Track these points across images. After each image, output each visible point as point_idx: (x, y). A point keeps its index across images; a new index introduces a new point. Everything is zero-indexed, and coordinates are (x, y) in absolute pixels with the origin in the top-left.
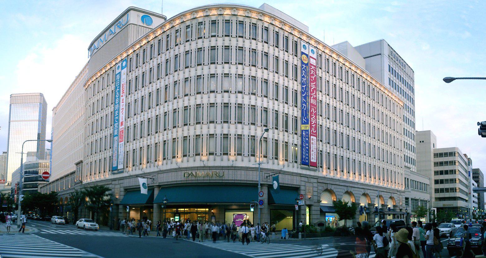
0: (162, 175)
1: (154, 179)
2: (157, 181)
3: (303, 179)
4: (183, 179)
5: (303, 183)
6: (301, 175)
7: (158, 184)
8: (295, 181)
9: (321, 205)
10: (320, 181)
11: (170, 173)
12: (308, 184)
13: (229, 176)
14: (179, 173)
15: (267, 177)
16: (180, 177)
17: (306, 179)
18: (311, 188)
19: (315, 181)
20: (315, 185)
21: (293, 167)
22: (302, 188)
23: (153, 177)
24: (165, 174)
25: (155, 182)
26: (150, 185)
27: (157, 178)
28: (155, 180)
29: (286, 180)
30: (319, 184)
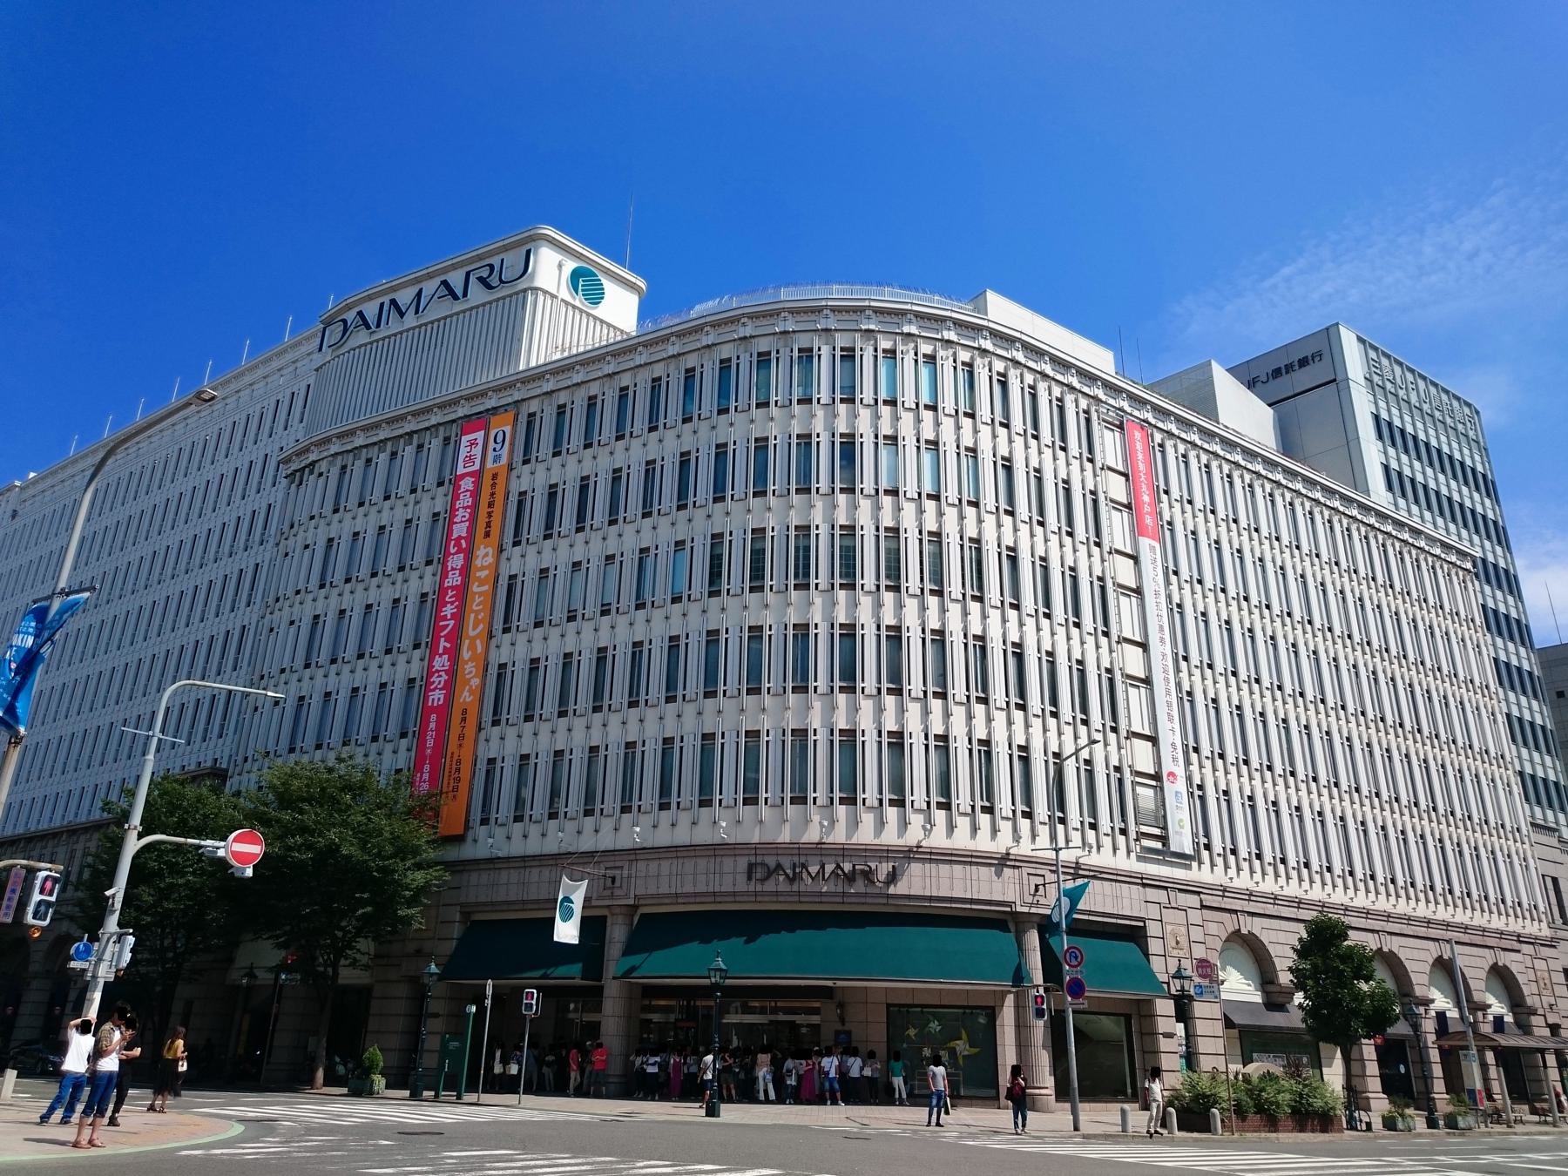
0: (653, 865)
1: (613, 879)
2: (628, 889)
3: (1153, 894)
4: (742, 885)
5: (1153, 912)
6: (1144, 882)
7: (631, 902)
8: (1126, 902)
9: (1224, 996)
10: (1209, 901)
11: (689, 865)
12: (1169, 915)
13: (917, 882)
14: (728, 863)
15: (1037, 886)
16: (728, 879)
17: (1161, 896)
18: (1183, 930)
19: (1193, 900)
20: (1195, 916)
21: (1115, 849)
22: (1153, 929)
23: (610, 873)
24: (665, 865)
25: (617, 892)
26: (594, 903)
27: (629, 877)
28: (617, 884)
29: (1100, 900)
30: (1208, 914)
